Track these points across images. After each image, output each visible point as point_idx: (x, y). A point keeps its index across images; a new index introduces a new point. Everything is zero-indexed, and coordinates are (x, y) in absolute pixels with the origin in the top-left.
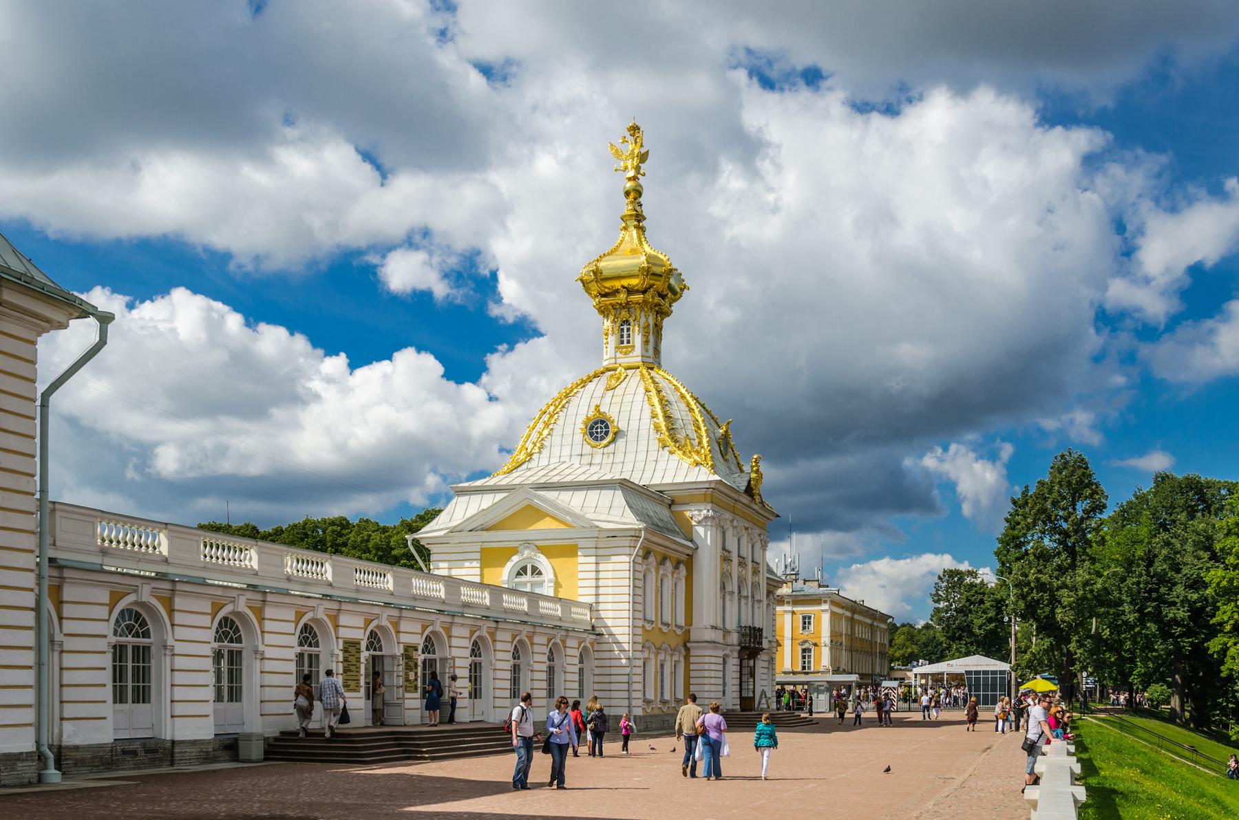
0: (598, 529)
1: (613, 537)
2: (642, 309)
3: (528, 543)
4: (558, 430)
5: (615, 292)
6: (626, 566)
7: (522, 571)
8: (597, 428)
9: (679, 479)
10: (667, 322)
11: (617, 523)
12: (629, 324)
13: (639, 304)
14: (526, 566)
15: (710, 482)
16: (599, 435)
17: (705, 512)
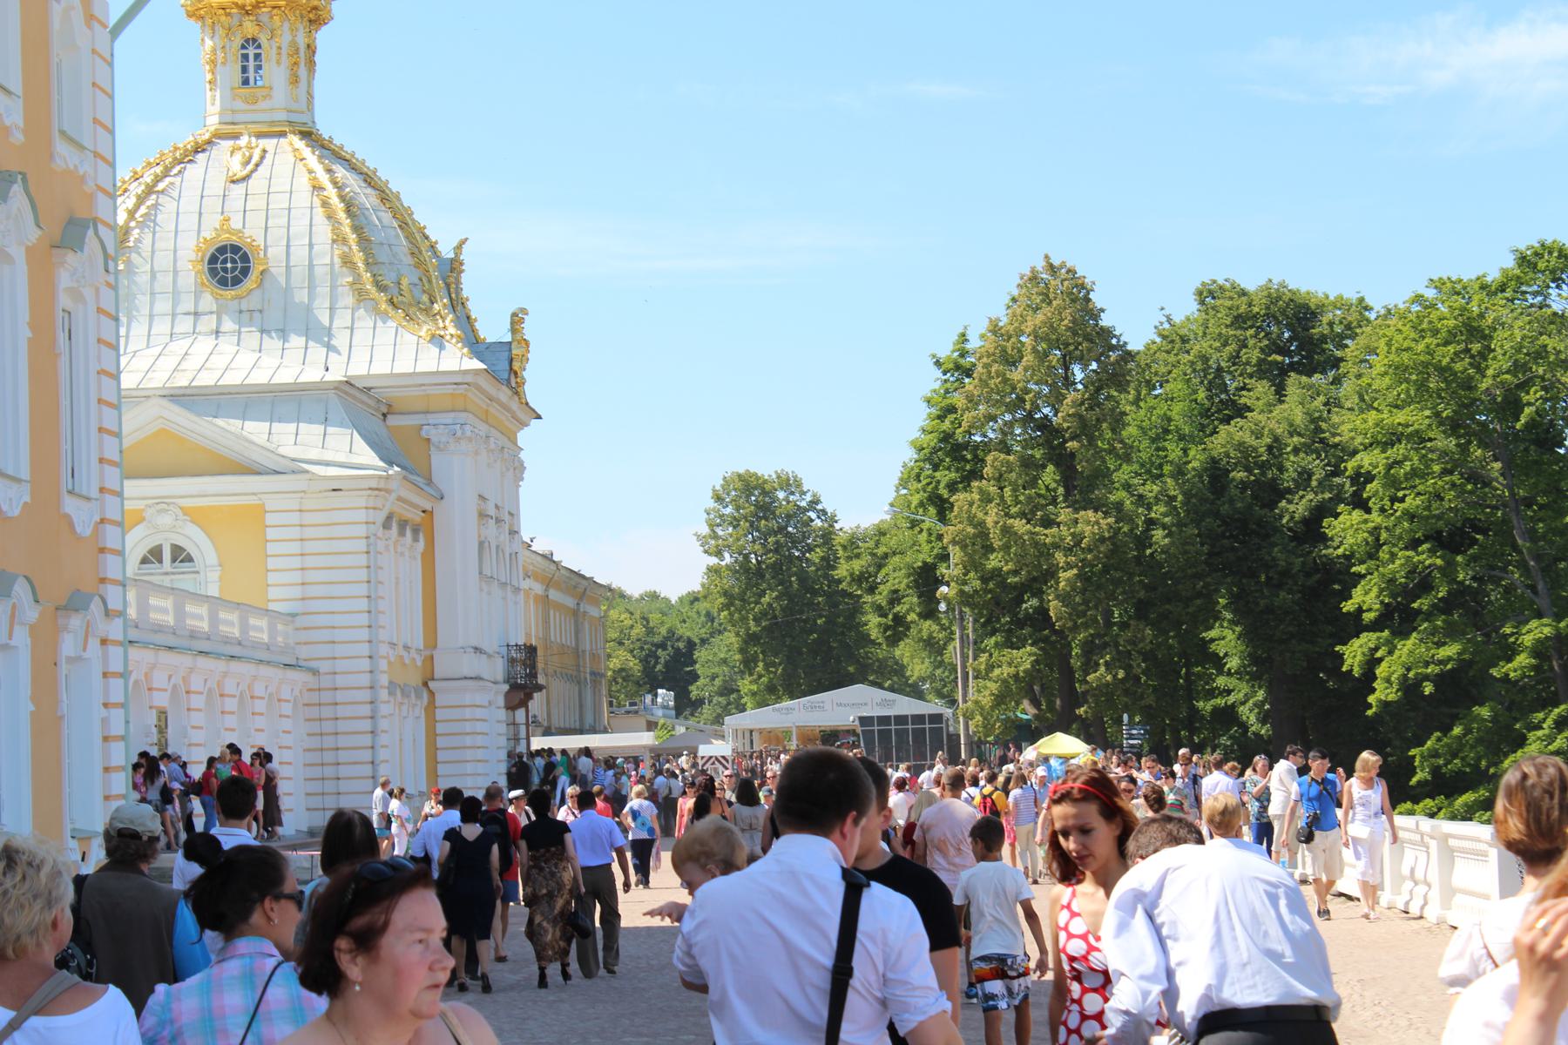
3: (163, 503)
6: (361, 545)
7: (155, 555)
8: (225, 261)
9: (404, 366)
10: (323, 36)
12: (259, 47)
14: (161, 546)
15: (466, 372)
16: (229, 276)
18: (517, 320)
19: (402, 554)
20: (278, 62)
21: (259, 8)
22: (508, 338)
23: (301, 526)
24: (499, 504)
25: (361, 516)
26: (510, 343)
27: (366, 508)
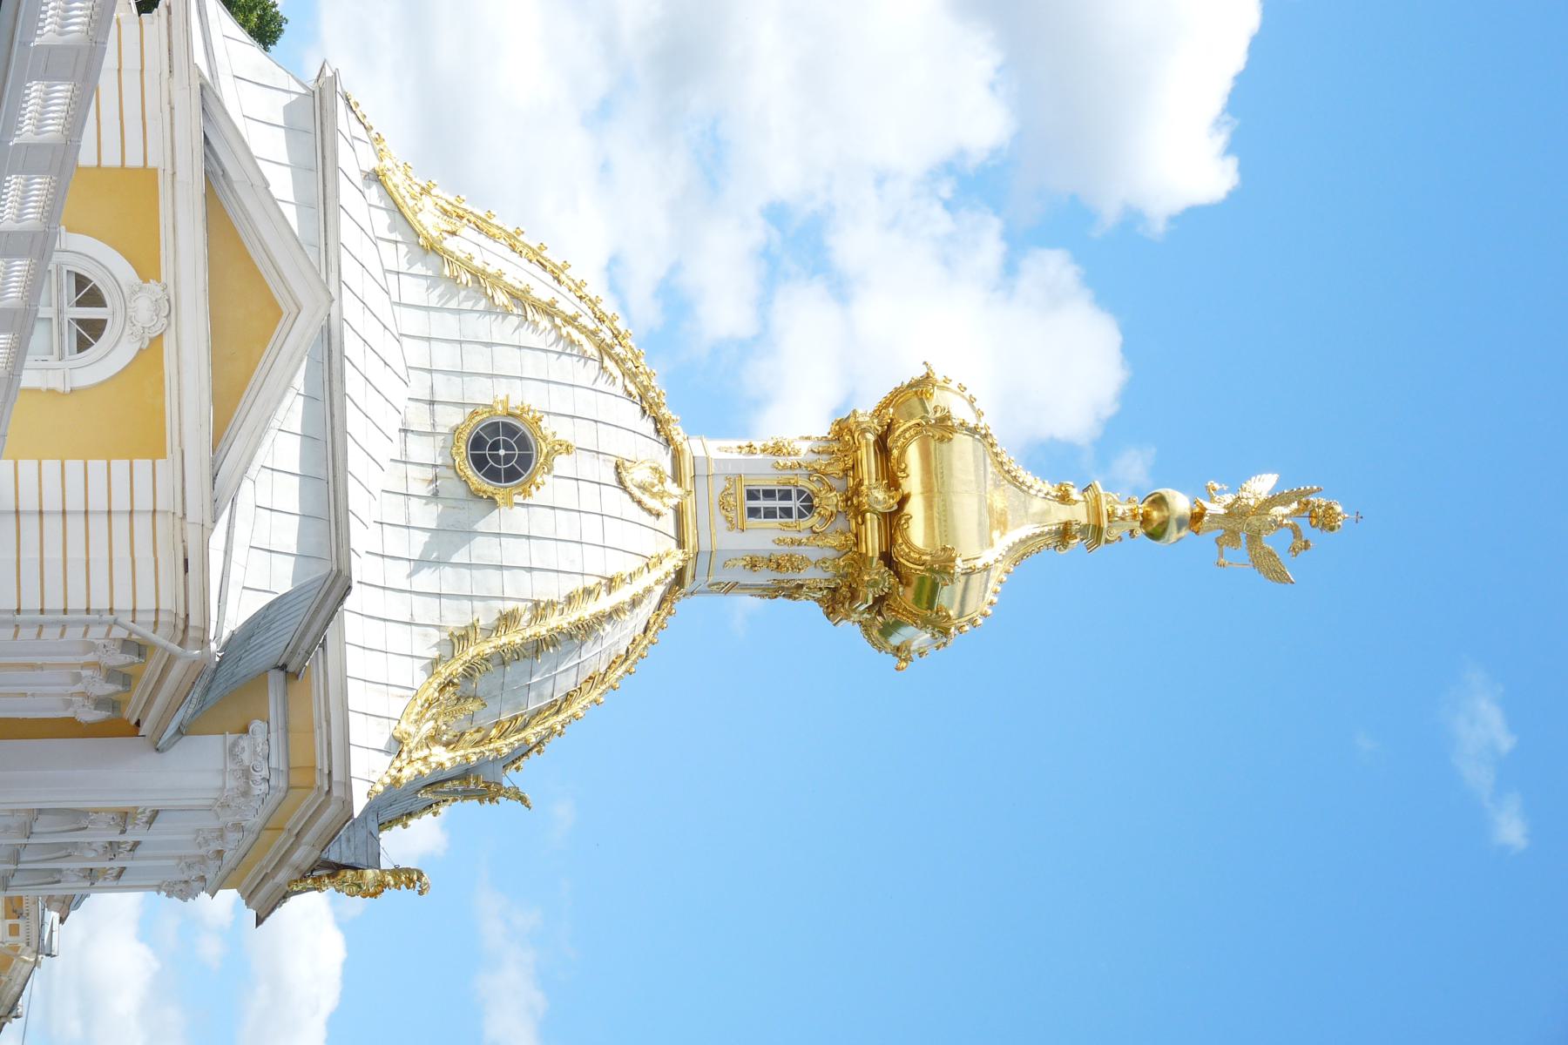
0: (208, 523)
1: (186, 561)
2: (843, 550)
3: (170, 309)
4: (503, 329)
5: (892, 481)
6: (100, 601)
7: (89, 294)
8: (508, 447)
9: (357, 696)
10: (809, 610)
11: (225, 575)
12: (801, 515)
13: (856, 544)
15: (347, 786)
17: (265, 773)
18: (408, 877)
19: (78, 678)
20: (780, 542)
21: (855, 517)
22: (385, 864)
23: (131, 512)
24: (139, 851)
25: (146, 602)
26: (379, 867)
27: (157, 610)
